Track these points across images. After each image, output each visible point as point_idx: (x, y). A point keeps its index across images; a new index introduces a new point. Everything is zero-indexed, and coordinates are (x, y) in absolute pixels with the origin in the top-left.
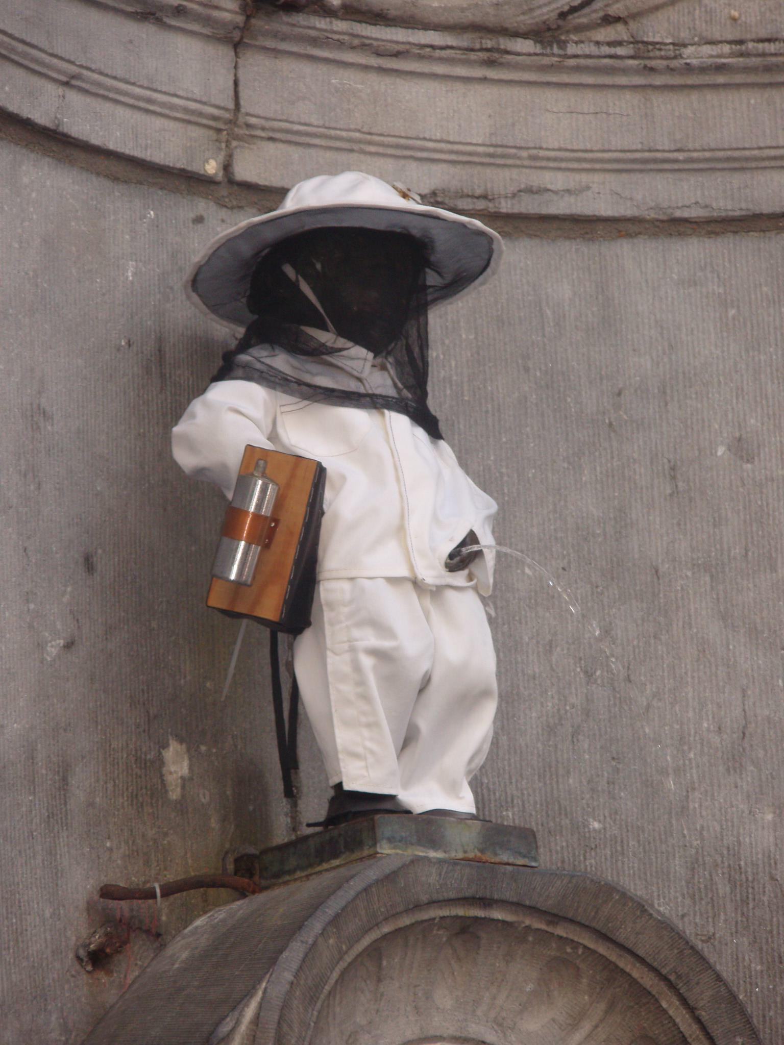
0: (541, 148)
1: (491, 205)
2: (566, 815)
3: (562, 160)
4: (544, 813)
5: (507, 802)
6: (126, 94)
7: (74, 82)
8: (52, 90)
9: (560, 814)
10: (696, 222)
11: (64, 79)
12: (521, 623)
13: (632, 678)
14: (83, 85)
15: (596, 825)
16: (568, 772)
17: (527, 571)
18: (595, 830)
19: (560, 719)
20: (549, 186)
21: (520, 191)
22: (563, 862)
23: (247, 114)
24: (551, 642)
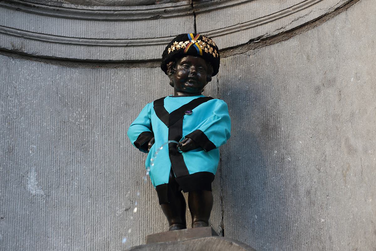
0: (295, 5)
1: (284, 29)
2: (314, 219)
3: (302, 6)
4: (307, 221)
5: (296, 221)
6: (152, 42)
7: (129, 45)
8: (123, 49)
9: (312, 220)
10: (342, 7)
11: (125, 45)
12: (299, 160)
13: (332, 166)
14: (134, 44)
15: (323, 220)
16: (314, 205)
17: (300, 142)
18: (323, 222)
19: (311, 187)
20: (301, 16)
21: (293, 21)
22: (313, 236)
23: (199, 33)
24: (308, 163)
